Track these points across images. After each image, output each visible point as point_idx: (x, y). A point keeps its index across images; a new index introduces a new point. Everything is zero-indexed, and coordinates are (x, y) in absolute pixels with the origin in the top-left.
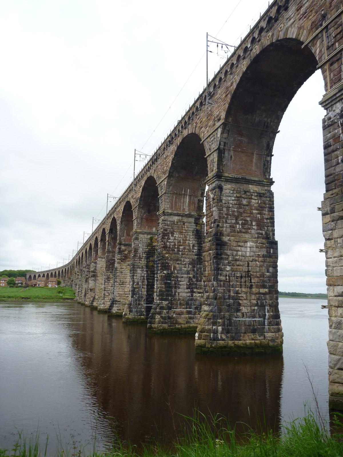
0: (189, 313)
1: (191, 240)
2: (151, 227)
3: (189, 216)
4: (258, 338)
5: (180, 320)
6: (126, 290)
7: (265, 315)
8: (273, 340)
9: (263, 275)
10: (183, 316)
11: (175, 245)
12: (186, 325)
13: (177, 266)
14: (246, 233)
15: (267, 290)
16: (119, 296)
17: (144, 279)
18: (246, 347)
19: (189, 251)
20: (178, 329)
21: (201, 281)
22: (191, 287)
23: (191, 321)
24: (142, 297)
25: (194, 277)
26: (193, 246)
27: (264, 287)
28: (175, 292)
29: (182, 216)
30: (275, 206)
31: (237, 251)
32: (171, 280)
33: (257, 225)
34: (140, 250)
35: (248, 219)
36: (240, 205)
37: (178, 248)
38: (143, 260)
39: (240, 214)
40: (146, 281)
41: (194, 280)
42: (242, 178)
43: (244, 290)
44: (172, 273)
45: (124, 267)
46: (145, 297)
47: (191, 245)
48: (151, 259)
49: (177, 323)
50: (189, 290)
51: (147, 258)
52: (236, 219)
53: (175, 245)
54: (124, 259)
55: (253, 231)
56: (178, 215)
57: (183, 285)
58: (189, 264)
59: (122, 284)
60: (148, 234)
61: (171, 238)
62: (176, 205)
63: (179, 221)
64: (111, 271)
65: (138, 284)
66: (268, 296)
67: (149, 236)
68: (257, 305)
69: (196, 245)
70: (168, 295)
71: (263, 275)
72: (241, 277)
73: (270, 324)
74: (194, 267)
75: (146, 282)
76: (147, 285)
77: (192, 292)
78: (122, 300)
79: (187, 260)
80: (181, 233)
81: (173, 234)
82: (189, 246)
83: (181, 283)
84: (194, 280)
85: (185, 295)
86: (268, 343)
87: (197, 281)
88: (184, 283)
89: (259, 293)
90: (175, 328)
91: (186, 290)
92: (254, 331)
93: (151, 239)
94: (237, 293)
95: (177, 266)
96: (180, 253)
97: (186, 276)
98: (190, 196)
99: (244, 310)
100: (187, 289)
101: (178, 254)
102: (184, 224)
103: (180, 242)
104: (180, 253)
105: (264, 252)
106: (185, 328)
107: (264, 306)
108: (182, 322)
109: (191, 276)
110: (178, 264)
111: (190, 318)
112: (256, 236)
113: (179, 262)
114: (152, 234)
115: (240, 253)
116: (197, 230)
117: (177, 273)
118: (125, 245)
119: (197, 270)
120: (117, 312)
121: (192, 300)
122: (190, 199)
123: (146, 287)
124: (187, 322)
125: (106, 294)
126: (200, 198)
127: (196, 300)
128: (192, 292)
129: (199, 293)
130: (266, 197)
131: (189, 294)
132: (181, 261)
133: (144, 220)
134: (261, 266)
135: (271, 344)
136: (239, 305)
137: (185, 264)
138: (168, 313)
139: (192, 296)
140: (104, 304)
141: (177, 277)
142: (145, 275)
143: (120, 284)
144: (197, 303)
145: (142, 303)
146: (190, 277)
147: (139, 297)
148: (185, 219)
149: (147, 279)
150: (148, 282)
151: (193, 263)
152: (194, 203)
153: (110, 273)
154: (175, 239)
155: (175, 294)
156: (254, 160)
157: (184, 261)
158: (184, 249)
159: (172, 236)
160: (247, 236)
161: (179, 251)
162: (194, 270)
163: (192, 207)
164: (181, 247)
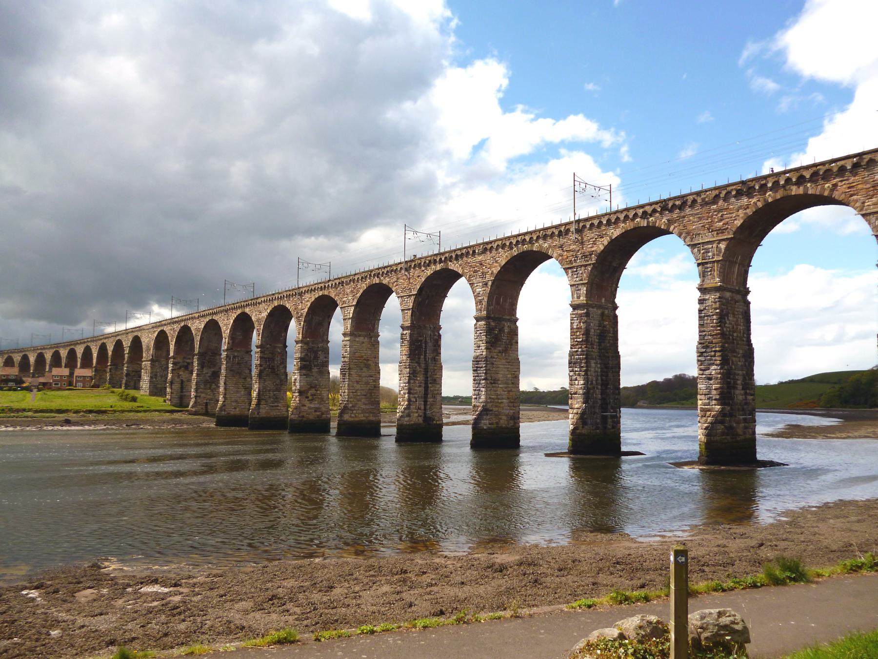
34: (592, 332)
46: (600, 402)
51: (600, 344)
60: (599, 307)
63: (732, 299)
65: (592, 383)
67: (599, 312)
75: (600, 381)
76: (602, 385)
78: (495, 409)
79: (741, 352)
93: (603, 314)
103: (733, 327)
118: (494, 319)
120: (489, 428)
124: (744, 433)
125: (413, 400)
138: (730, 421)
140: (409, 415)
143: (491, 383)
145: (597, 411)
149: (602, 375)
164: (735, 334)
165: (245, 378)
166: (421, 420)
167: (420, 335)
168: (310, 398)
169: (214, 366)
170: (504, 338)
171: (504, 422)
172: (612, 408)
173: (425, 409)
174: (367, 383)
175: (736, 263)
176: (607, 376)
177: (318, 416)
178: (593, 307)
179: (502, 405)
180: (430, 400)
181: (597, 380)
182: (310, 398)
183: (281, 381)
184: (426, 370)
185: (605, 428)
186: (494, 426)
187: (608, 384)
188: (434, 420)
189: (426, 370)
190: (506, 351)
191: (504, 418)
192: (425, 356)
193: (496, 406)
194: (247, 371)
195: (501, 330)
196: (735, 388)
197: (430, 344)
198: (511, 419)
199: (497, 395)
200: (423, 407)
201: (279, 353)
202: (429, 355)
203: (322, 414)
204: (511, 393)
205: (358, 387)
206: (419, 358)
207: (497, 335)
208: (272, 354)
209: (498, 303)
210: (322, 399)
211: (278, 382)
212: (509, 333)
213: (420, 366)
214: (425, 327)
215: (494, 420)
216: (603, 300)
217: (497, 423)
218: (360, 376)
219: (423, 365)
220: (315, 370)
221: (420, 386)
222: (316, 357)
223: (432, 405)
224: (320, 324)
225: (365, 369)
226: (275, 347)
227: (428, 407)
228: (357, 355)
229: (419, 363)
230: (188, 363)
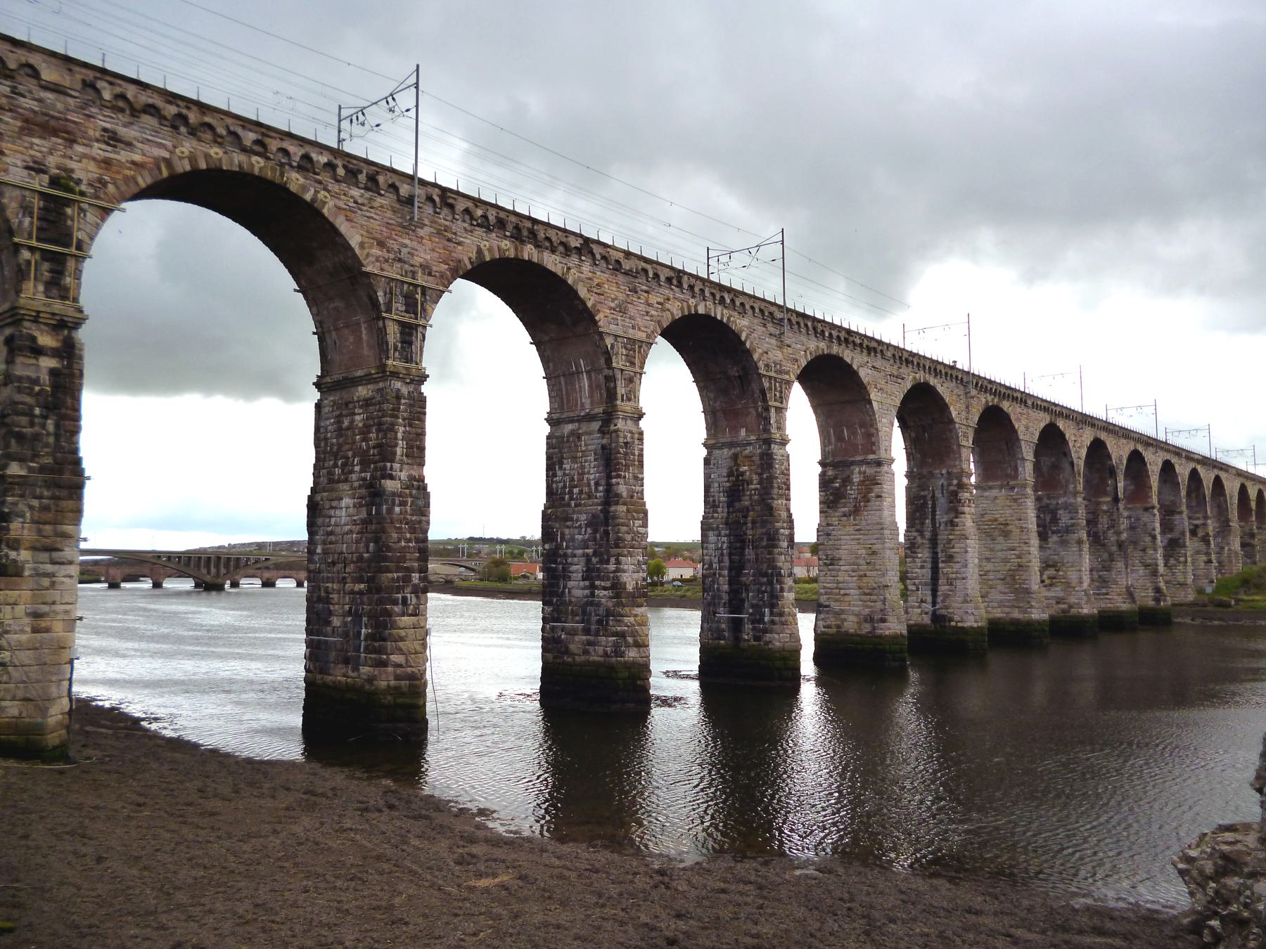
0: (587, 631)
1: (593, 473)
2: (735, 429)
3: (590, 418)
4: (351, 673)
5: (572, 647)
6: (840, 579)
7: (359, 633)
8: (371, 680)
9: (360, 559)
10: (577, 638)
11: (565, 487)
12: (583, 658)
13: (567, 531)
14: (346, 480)
15: (362, 586)
16: (826, 594)
17: (722, 554)
18: (336, 687)
19: (590, 496)
20: (568, 664)
21: (608, 562)
22: (591, 574)
23: (591, 649)
24: (720, 598)
25: (595, 554)
26: (597, 484)
27: (360, 580)
28: (565, 587)
29: (579, 421)
30: (427, 410)
31: (330, 517)
32: (555, 562)
33: (361, 463)
35: (350, 454)
36: (340, 431)
37: (571, 492)
38: (720, 510)
39: (340, 446)
40: (726, 559)
41: (594, 560)
42: (345, 379)
43: (335, 586)
44: (559, 547)
45: (835, 521)
46: (725, 597)
47: (592, 483)
48: (737, 505)
49: (567, 652)
50: (587, 583)
51: (730, 504)
52: (336, 459)
53: (565, 487)
54: (832, 502)
55: (354, 477)
56: (571, 421)
57: (576, 572)
58: (587, 526)
59: (831, 564)
60: (731, 445)
61: (559, 473)
62: (568, 399)
63: (572, 433)
64: (919, 527)
66: (365, 598)
68: (349, 613)
69: (603, 482)
70: (552, 594)
71: (360, 559)
72: (334, 563)
73: (366, 648)
74: (595, 531)
76: (730, 569)
77: (593, 587)
79: (583, 517)
80: (574, 459)
81: (561, 463)
82: (589, 485)
83: (574, 568)
84: (594, 560)
85: (578, 593)
86: (363, 686)
87: (601, 562)
88: (578, 568)
89: (352, 592)
90: (564, 663)
91: (582, 583)
92: (346, 661)
93: (735, 457)
94: (327, 591)
95: (567, 531)
96: (573, 503)
97: (580, 552)
98: (588, 372)
99: (336, 621)
100: (583, 580)
101: (569, 505)
102: (579, 438)
103: (573, 480)
104: (573, 503)
105: (364, 515)
106: (582, 665)
107: (361, 616)
108: (576, 651)
109: (590, 551)
110: (568, 527)
111: (590, 643)
112: (356, 484)
113: (569, 523)
114: (738, 445)
115: (333, 520)
116: (603, 447)
117: (567, 547)
118: (835, 465)
119: (602, 539)
121: (591, 604)
122: (590, 378)
123: (726, 572)
126: (606, 372)
127: (599, 605)
128: (593, 587)
129: (605, 589)
130: (375, 404)
131: (587, 592)
132: (572, 519)
133: (720, 415)
134: (358, 542)
135: (367, 687)
136: (330, 613)
137: (580, 526)
139: (593, 595)
141: (565, 555)
142: (725, 546)
143: (825, 564)
144: (601, 611)
146: (587, 555)
147: (713, 597)
148: (584, 427)
149: (730, 554)
150: (731, 561)
151: (593, 523)
152: (598, 387)
153: (915, 534)
154: (565, 474)
155: (563, 592)
156: (364, 337)
157: (577, 520)
158: (581, 492)
159: (561, 468)
160: (346, 486)
161: (571, 499)
162: (595, 539)
163: (597, 396)
164: (576, 490)
165: (1144, 550)
166: (927, 620)
167: (922, 487)
168: (1047, 582)
169: (1171, 530)
170: (852, 492)
171: (851, 625)
172: (753, 606)
173: (934, 603)
174: (1006, 561)
175: (579, 373)
176: (742, 554)
177: (1063, 611)
178: (721, 448)
179: (847, 598)
180: (943, 588)
181: (720, 562)
182: (1047, 582)
183: (1111, 555)
184: (934, 542)
185: (737, 639)
186: (834, 630)
187: (743, 568)
188: (951, 620)
189: (934, 542)
190: (856, 511)
191: (852, 618)
192: (933, 520)
193: (836, 601)
194: (1148, 539)
195: (847, 481)
196: (566, 575)
197: (942, 501)
198: (866, 621)
199: (838, 582)
200: (929, 599)
201: (1105, 512)
202: (941, 517)
203: (1071, 607)
204: (865, 580)
205: (989, 566)
206: (923, 524)
207: (837, 489)
208: (1093, 513)
209: (840, 438)
210: (1068, 585)
211: (1105, 556)
212: (862, 483)
213: (922, 536)
214: (932, 475)
215: (832, 621)
216: (743, 432)
217: (838, 627)
218: (992, 550)
219: (928, 535)
220: (1054, 538)
221: (922, 567)
222: (1055, 520)
223: (946, 596)
224: (1056, 467)
225: (1001, 539)
226: (1098, 504)
227: (939, 599)
228: (987, 518)
229: (921, 533)
230: (1197, 526)
